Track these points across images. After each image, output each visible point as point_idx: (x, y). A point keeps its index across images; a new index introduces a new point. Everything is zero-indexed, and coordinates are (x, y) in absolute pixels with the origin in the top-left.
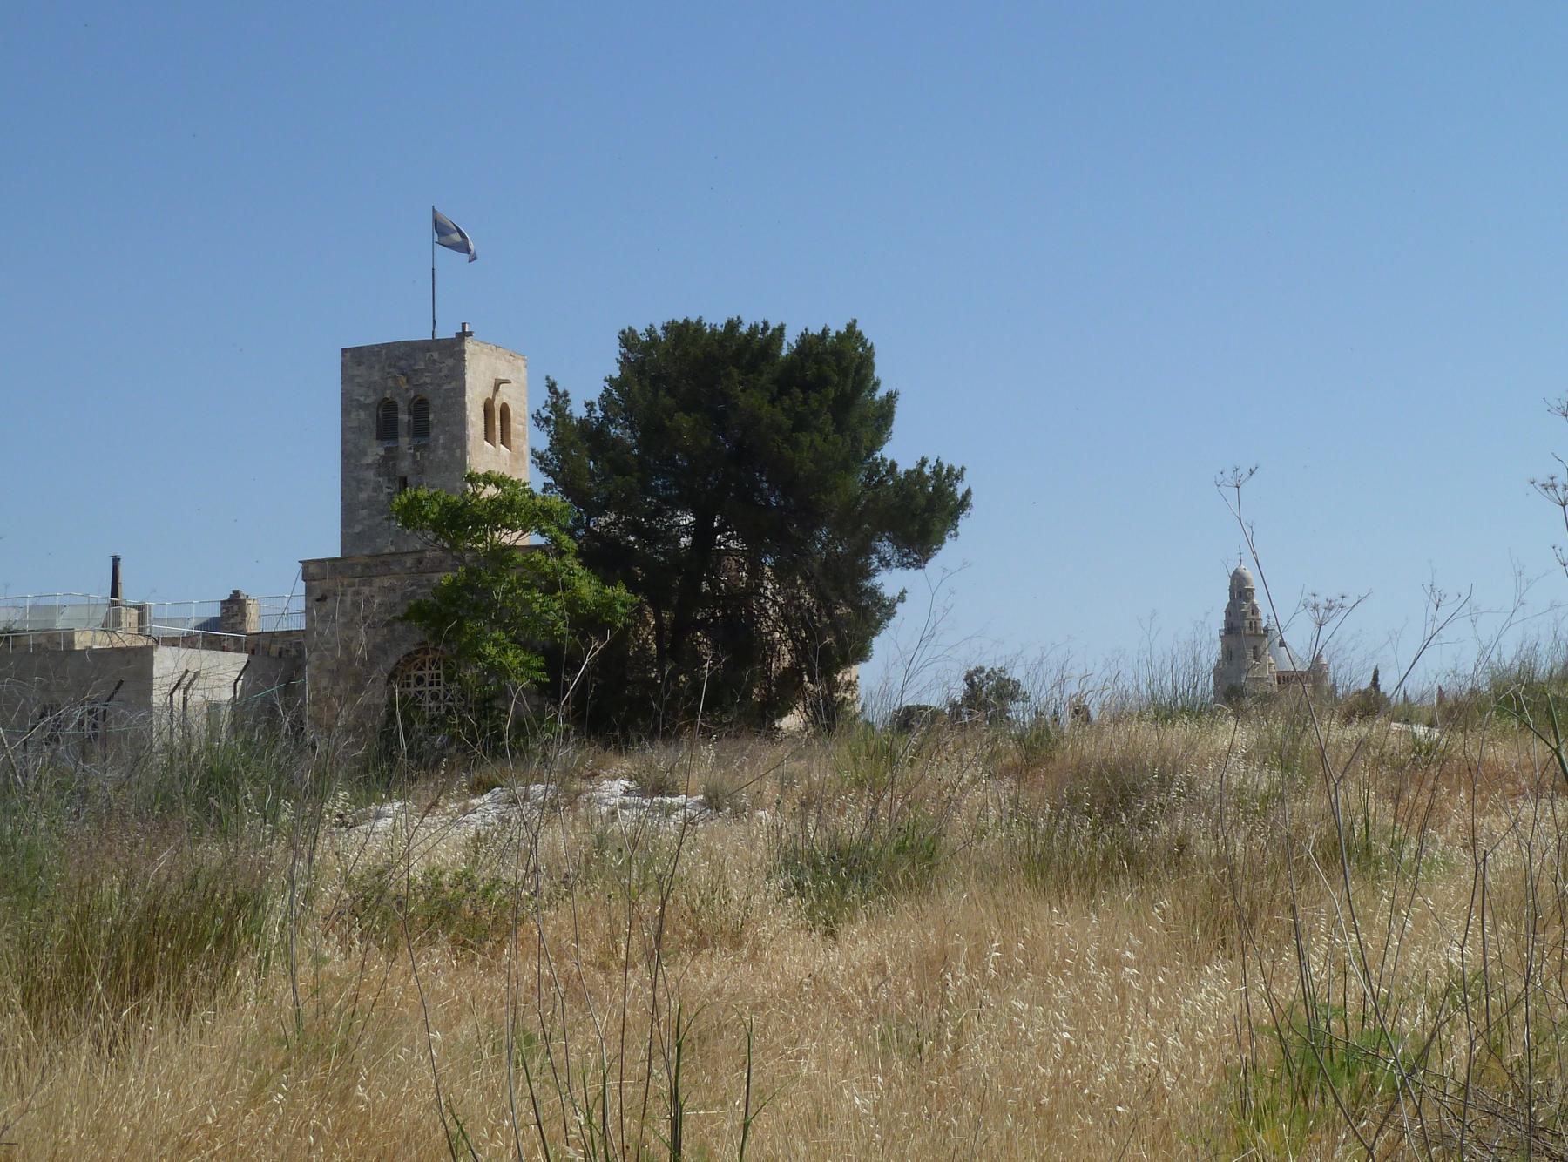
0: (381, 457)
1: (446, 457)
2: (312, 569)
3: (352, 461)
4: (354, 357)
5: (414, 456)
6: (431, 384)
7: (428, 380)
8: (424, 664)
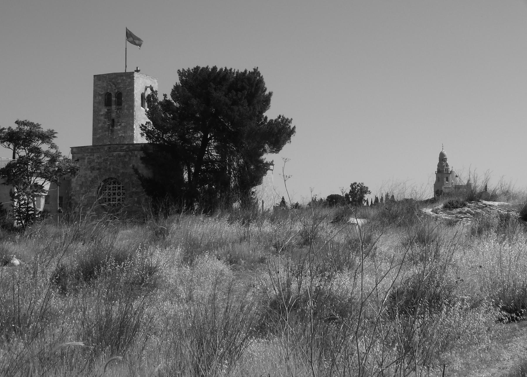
0: (106, 112)
1: (127, 112)
2: (74, 150)
3: (97, 113)
4: (98, 78)
5: (117, 112)
6: (123, 88)
7: (122, 86)
8: (111, 183)
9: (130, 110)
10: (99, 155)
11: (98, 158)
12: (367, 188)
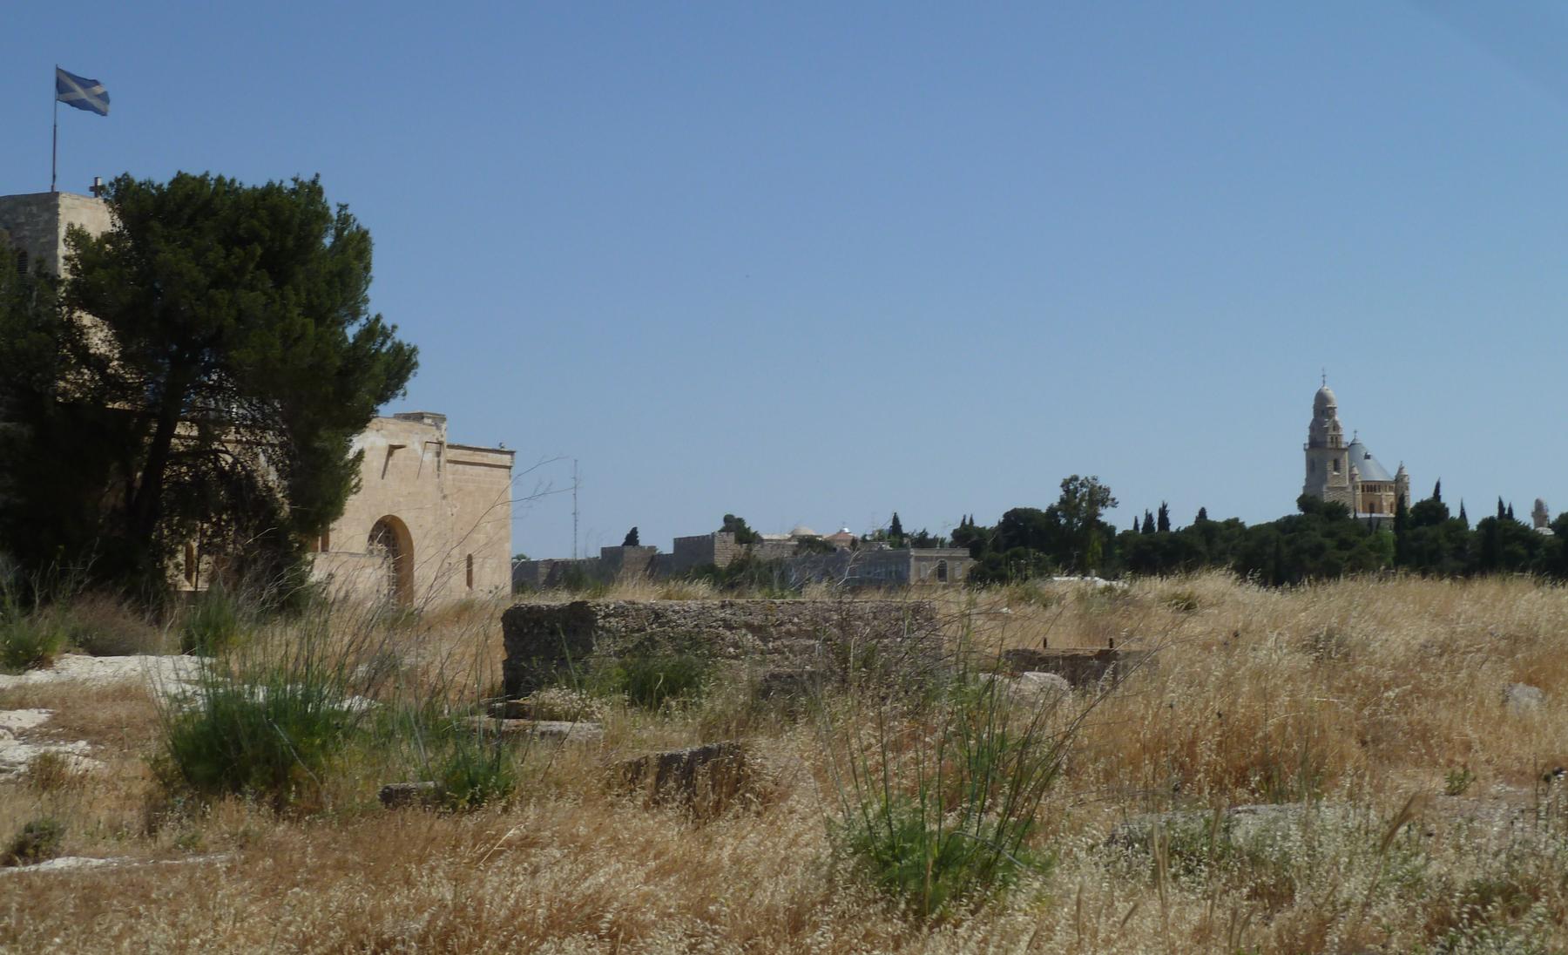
7: (27, 233)
12: (1107, 490)
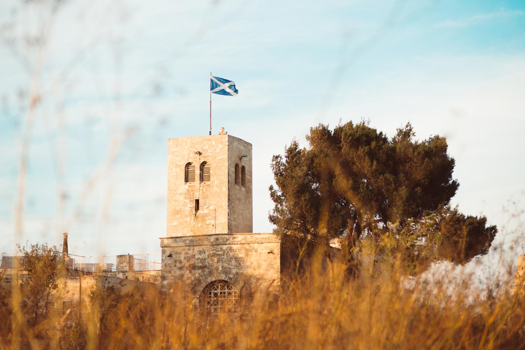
0: (187, 190)
6: (211, 156)
7: (210, 155)
8: (218, 288)
9: (222, 187)
10: (201, 249)
11: (200, 253)
